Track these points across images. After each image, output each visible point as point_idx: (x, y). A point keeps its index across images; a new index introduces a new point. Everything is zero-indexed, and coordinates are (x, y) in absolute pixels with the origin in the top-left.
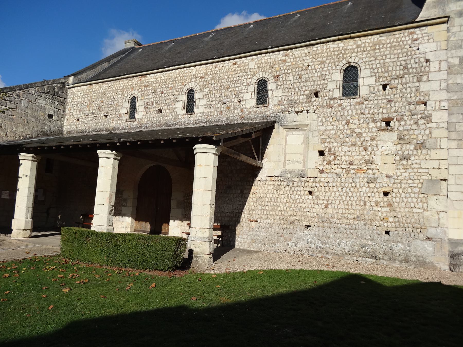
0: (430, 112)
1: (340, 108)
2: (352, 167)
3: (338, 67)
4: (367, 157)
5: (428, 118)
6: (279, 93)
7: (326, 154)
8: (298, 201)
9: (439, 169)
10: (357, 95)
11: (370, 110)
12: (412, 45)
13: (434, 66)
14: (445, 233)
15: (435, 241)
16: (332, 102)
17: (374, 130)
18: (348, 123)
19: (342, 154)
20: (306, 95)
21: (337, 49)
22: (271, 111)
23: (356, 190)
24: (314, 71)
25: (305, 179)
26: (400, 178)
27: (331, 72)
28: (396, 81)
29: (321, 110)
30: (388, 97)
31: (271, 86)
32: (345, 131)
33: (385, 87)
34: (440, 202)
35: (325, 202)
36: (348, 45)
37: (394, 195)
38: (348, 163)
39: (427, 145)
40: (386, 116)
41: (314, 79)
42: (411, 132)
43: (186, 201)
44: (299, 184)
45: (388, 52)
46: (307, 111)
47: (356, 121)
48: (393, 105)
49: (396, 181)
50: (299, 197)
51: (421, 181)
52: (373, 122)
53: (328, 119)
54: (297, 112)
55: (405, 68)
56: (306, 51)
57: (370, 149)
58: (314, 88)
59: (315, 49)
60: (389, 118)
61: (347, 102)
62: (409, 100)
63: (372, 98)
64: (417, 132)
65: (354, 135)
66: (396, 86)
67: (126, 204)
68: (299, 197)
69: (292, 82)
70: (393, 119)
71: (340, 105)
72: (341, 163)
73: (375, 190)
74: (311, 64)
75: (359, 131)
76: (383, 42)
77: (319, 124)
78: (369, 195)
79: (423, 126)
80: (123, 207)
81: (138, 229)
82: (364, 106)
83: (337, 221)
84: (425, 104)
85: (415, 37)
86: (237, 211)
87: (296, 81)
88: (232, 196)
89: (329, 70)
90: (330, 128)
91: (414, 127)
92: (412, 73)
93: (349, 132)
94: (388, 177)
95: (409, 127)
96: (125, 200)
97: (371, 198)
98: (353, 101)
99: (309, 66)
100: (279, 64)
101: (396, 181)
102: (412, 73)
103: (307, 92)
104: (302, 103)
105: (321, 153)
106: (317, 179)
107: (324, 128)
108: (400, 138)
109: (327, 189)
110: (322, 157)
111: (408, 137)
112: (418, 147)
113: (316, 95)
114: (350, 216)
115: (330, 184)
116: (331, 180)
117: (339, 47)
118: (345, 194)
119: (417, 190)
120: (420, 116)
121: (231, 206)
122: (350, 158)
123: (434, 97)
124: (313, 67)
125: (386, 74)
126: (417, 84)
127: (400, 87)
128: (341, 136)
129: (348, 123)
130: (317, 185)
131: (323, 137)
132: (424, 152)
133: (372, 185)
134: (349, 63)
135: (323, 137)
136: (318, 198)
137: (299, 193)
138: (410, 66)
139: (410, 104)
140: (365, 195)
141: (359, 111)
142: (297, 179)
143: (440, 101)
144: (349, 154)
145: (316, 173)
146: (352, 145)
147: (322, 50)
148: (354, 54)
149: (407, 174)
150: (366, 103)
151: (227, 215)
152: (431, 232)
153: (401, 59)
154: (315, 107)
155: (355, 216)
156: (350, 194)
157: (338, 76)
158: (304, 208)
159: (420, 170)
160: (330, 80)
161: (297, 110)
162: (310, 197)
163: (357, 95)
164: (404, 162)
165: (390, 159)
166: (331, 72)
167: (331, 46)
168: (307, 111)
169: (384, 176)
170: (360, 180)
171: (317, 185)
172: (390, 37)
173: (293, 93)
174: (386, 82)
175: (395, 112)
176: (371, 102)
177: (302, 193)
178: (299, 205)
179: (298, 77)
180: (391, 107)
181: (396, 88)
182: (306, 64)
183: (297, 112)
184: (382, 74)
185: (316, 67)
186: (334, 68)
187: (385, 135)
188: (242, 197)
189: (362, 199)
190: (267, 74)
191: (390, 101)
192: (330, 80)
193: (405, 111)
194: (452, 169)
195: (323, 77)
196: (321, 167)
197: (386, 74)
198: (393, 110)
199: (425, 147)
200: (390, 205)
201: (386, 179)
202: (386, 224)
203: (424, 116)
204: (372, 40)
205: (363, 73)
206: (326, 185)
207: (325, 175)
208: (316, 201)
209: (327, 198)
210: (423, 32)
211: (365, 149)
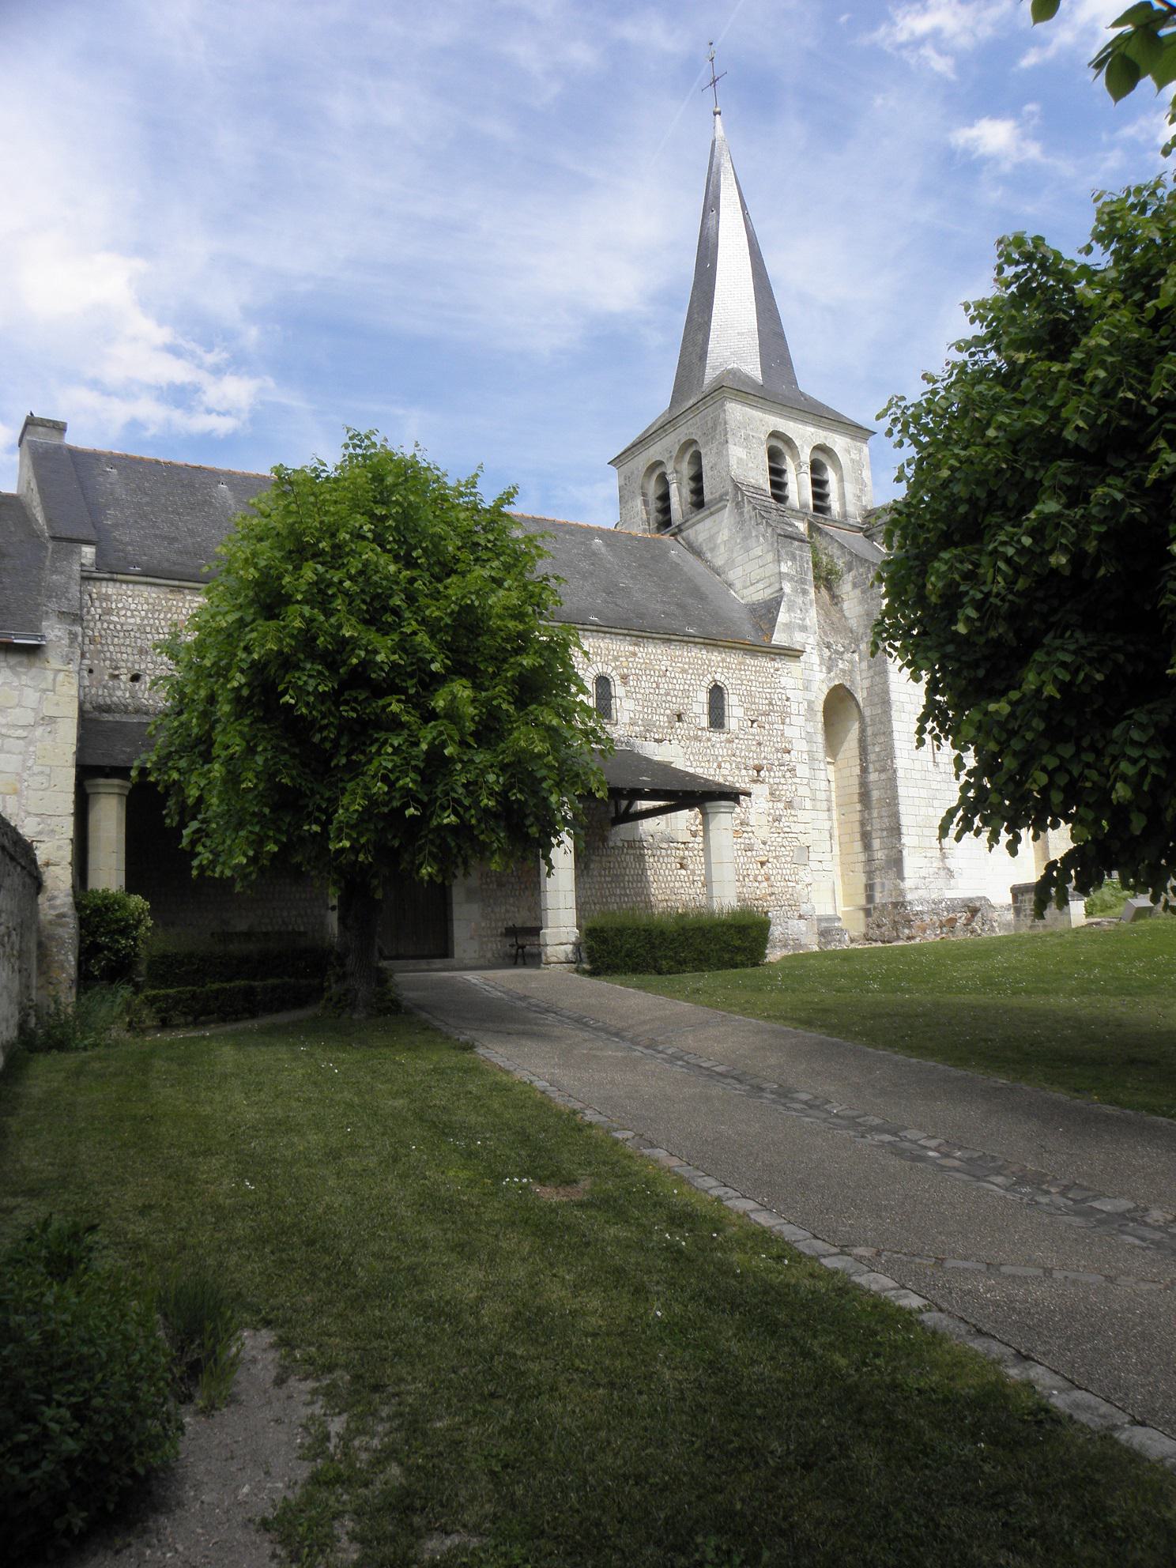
4: (742, 816)
6: (629, 704)
13: (794, 708)
14: (814, 908)
16: (700, 733)
17: (747, 779)
18: (719, 767)
22: (621, 732)
31: (618, 690)
39: (795, 805)
40: (756, 762)
42: (780, 787)
43: (484, 886)
47: (728, 765)
54: (656, 740)
55: (771, 704)
61: (716, 737)
64: (785, 787)
69: (647, 692)
71: (709, 740)
74: (670, 669)
84: (789, 752)
87: (652, 691)
91: (783, 781)
92: (777, 712)
94: (764, 843)
98: (724, 737)
100: (627, 657)
102: (777, 712)
103: (668, 712)
104: (663, 728)
106: (690, 845)
108: (772, 794)
119: (789, 859)
125: (753, 707)
126: (781, 727)
129: (719, 767)
133: (749, 853)
136: (693, 873)
139: (777, 751)
142: (665, 845)
145: (688, 838)
148: (720, 670)
149: (779, 840)
150: (736, 741)
152: (804, 908)
157: (704, 697)
161: (657, 737)
162: (683, 872)
164: (776, 824)
165: (764, 819)
175: (765, 758)
178: (672, 885)
179: (654, 685)
180: (761, 752)
182: (664, 668)
183: (656, 740)
190: (610, 668)
191: (760, 744)
196: (694, 828)
197: (753, 707)
200: (768, 879)
201: (762, 846)
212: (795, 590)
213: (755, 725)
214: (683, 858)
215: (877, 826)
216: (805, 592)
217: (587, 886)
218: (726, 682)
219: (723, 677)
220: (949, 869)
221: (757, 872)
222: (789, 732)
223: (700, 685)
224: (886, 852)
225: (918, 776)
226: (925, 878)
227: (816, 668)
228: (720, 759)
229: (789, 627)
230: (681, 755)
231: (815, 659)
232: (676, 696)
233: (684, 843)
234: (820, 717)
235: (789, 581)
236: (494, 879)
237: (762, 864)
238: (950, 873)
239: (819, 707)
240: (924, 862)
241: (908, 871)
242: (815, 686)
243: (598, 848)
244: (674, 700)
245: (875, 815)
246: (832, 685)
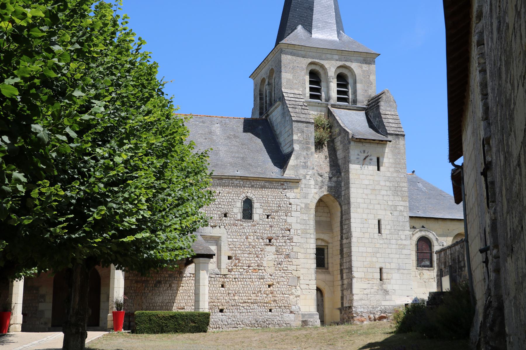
0: (292, 236)
1: (242, 227)
2: (250, 268)
3: (240, 198)
5: (291, 239)
7: (234, 257)
8: (215, 292)
9: (296, 271)
10: (251, 219)
11: (260, 230)
12: (283, 193)
14: (299, 308)
15: (294, 314)
16: (236, 222)
17: (263, 244)
18: (247, 238)
19: (244, 259)
20: (219, 215)
21: (239, 185)
23: (252, 284)
24: (224, 198)
25: (219, 276)
26: (277, 275)
27: (235, 200)
28: (275, 214)
29: (229, 227)
30: (270, 223)
32: (245, 243)
33: (268, 216)
34: (297, 290)
35: (234, 292)
36: (246, 184)
37: (274, 286)
38: (247, 265)
40: (269, 235)
41: (224, 203)
44: (216, 279)
45: (269, 194)
46: (220, 226)
47: (252, 237)
48: (273, 228)
49: (275, 278)
50: (216, 289)
51: (288, 278)
52: (262, 239)
53: (234, 234)
55: (279, 206)
56: (218, 182)
57: (260, 256)
58: (224, 211)
59: (224, 182)
60: (271, 237)
61: (247, 224)
62: (281, 227)
63: (261, 223)
65: (251, 246)
66: (274, 217)
68: (216, 289)
70: (273, 238)
72: (243, 265)
73: (264, 283)
74: (221, 192)
75: (254, 244)
76: (267, 186)
77: (228, 237)
78: (260, 287)
79: (289, 244)
80: (40, 304)
82: (256, 227)
83: (241, 305)
84: (289, 230)
85: (284, 187)
86: (167, 301)
88: (162, 289)
89: (234, 199)
90: (236, 240)
91: (284, 244)
93: (248, 244)
94: (271, 275)
95: (281, 244)
96: (43, 296)
97: (261, 289)
99: (220, 193)
101: (275, 278)
103: (219, 212)
105: (229, 258)
106: (228, 276)
107: (232, 240)
109: (234, 283)
110: (230, 260)
111: (281, 250)
112: (286, 257)
113: (225, 215)
114: (249, 301)
115: (237, 280)
116: (237, 276)
117: (240, 184)
118: (246, 286)
119: (286, 283)
120: (287, 238)
121: (162, 298)
122: (248, 262)
123: (295, 226)
124: (223, 195)
125: (269, 208)
126: (285, 218)
127: (276, 218)
128: (243, 247)
129: (247, 238)
130: (228, 280)
131: (230, 246)
132: (290, 260)
133: (262, 280)
134: (247, 197)
135: (230, 246)
136: (229, 289)
137: (215, 286)
138: (281, 206)
140: (258, 287)
141: (253, 231)
143: (297, 230)
144: (248, 259)
146: (250, 254)
147: (229, 183)
151: (158, 305)
152: (293, 308)
153: (277, 200)
154: (225, 224)
155: (252, 301)
156: (249, 286)
158: (219, 297)
159: (287, 271)
160: (235, 206)
161: (212, 224)
162: (223, 289)
163: (251, 219)
164: (279, 266)
165: (271, 264)
166: (235, 200)
167: (235, 182)
168: (220, 226)
169: (268, 274)
170: (254, 276)
171: (228, 280)
172: (270, 184)
173: (209, 212)
174: (268, 214)
176: (261, 225)
177: (218, 285)
181: (274, 218)
184: (266, 208)
185: (225, 194)
186: (237, 198)
187: (269, 248)
188: (170, 290)
189: (256, 289)
192: (235, 206)
193: (280, 233)
194: (302, 271)
195: (229, 204)
196: (230, 268)
197: (269, 208)
198: (273, 232)
199: (289, 258)
200: (272, 293)
201: (269, 277)
202: (270, 305)
203: (289, 238)
204: (261, 184)
205: (256, 205)
206: (234, 280)
207: (233, 273)
208: (227, 291)
209: (234, 289)
210: (288, 185)
211: (257, 257)
212: (303, 149)
213: (270, 217)
214: (223, 282)
215: (345, 267)
216: (308, 149)
217: (170, 295)
218: (254, 197)
219: (252, 195)
220: (385, 290)
221: (265, 289)
222: (289, 220)
223: (238, 199)
224: (347, 280)
225: (367, 241)
226: (367, 295)
227: (312, 187)
228: (247, 234)
229: (296, 167)
230: (226, 233)
231: (312, 182)
232: (224, 205)
233: (225, 275)
234: (313, 211)
235: (298, 144)
237: (269, 286)
238: (386, 292)
239: (313, 206)
240: (365, 286)
241: (354, 291)
242: (310, 196)
243: (177, 277)
244: (223, 206)
245: (344, 261)
246: (322, 195)
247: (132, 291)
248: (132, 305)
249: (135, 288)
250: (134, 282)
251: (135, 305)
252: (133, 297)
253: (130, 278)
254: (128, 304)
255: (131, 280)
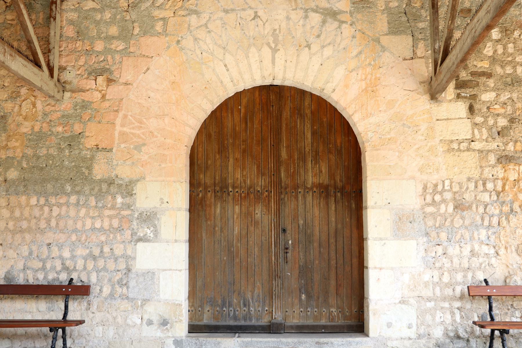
43: (430, 209)
67: (156, 233)
80: (140, 245)
81: (206, 320)
236: (448, 196)
247: (486, 197)
248: (492, 251)
249: (500, 183)
250: (492, 159)
251: (502, 252)
252: (495, 220)
253: (476, 145)
254: (477, 247)
255: (480, 151)
